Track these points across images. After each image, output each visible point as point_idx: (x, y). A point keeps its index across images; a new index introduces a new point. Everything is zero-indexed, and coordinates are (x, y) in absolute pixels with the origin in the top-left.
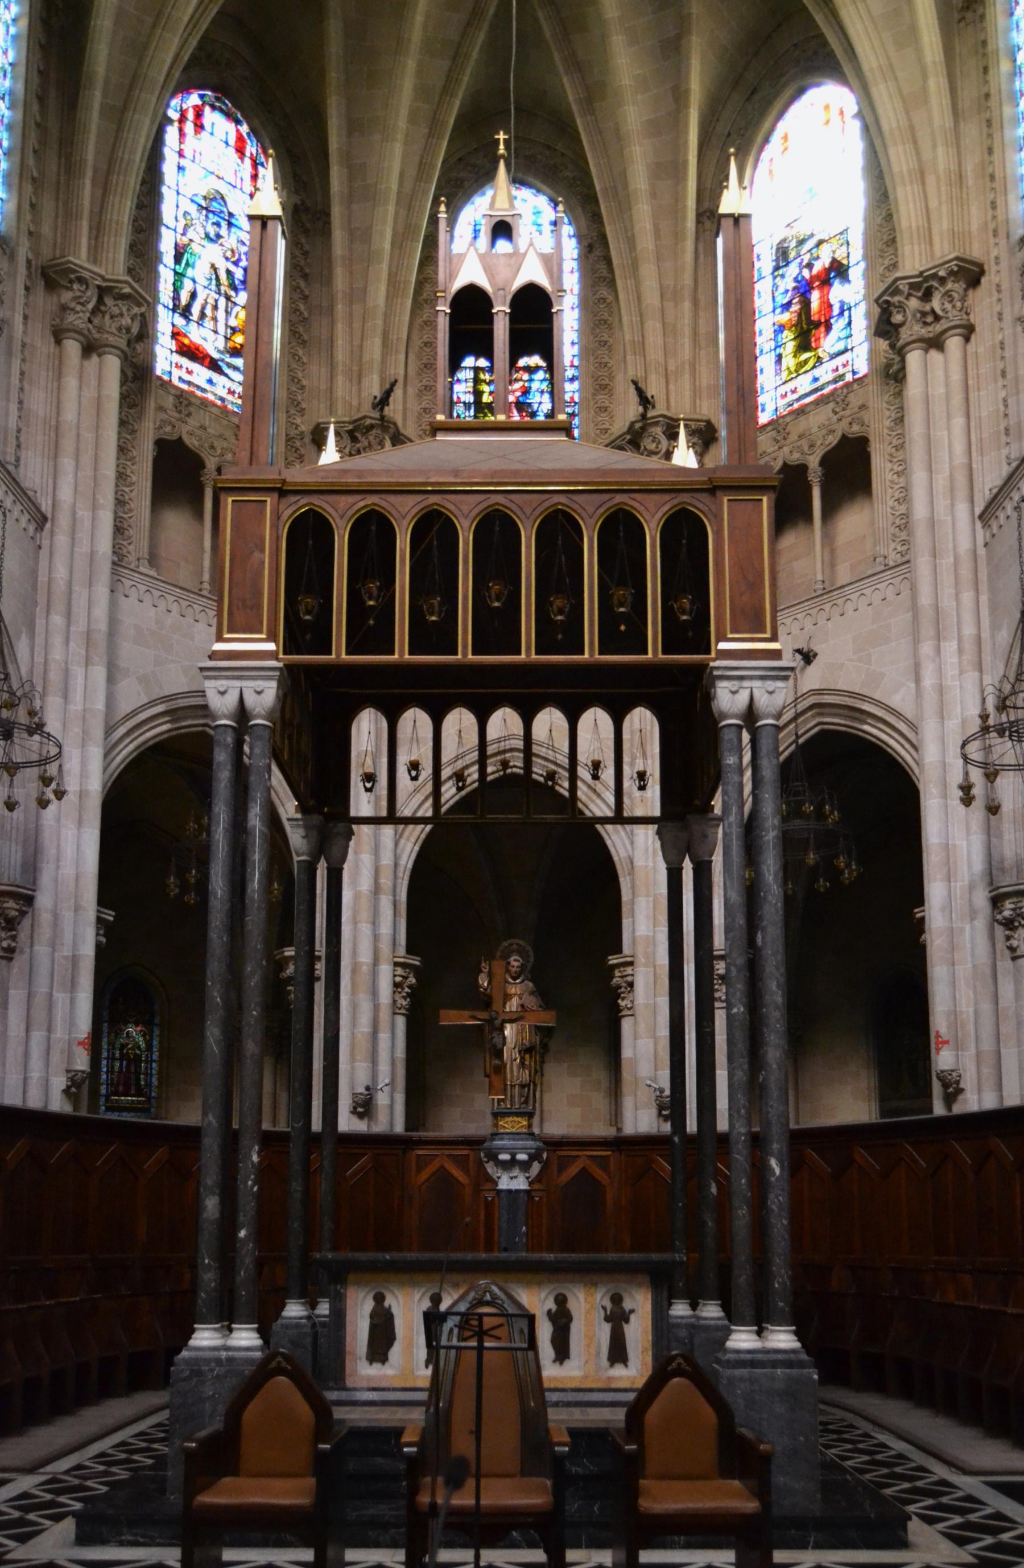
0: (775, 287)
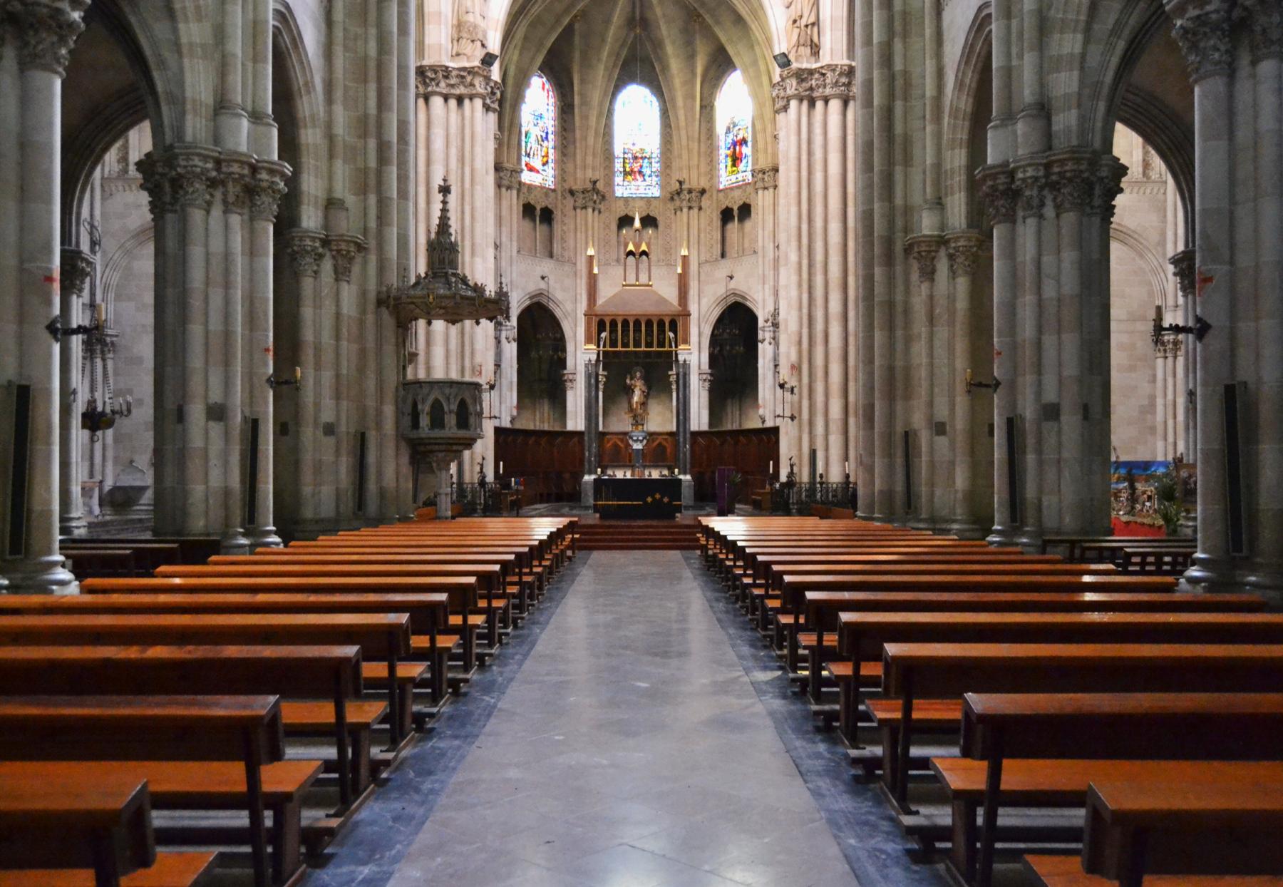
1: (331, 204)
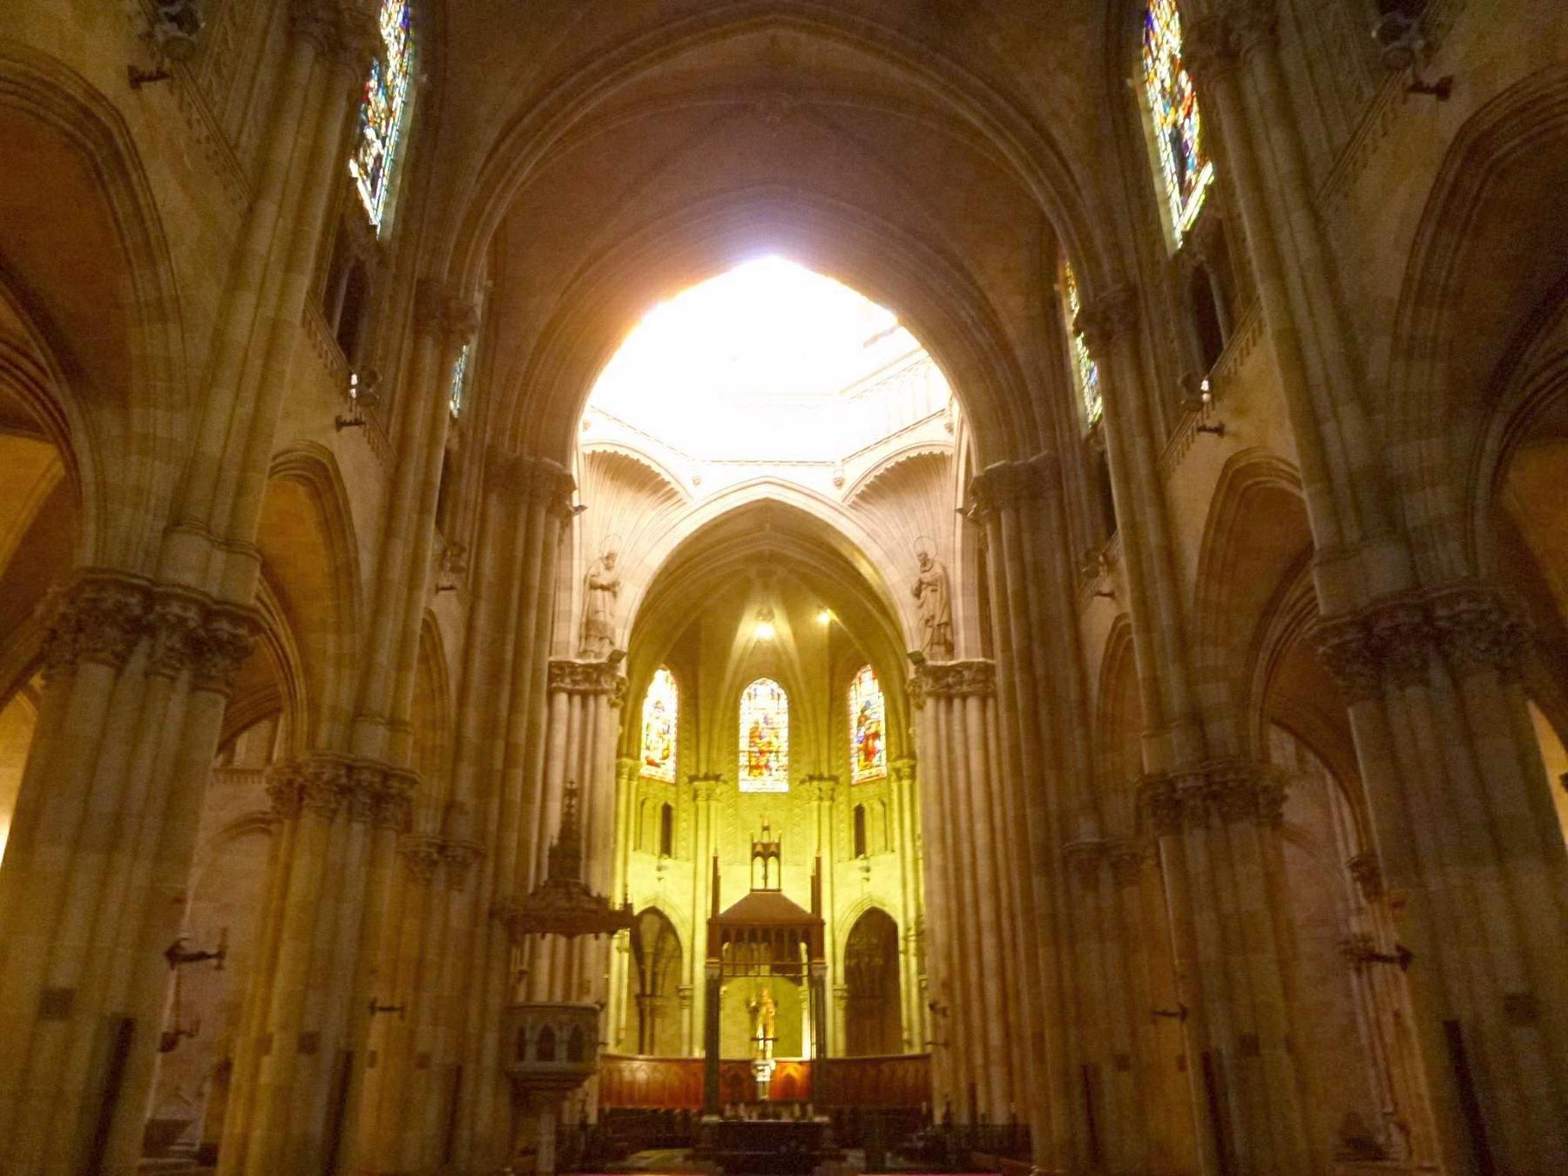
1: (451, 807)
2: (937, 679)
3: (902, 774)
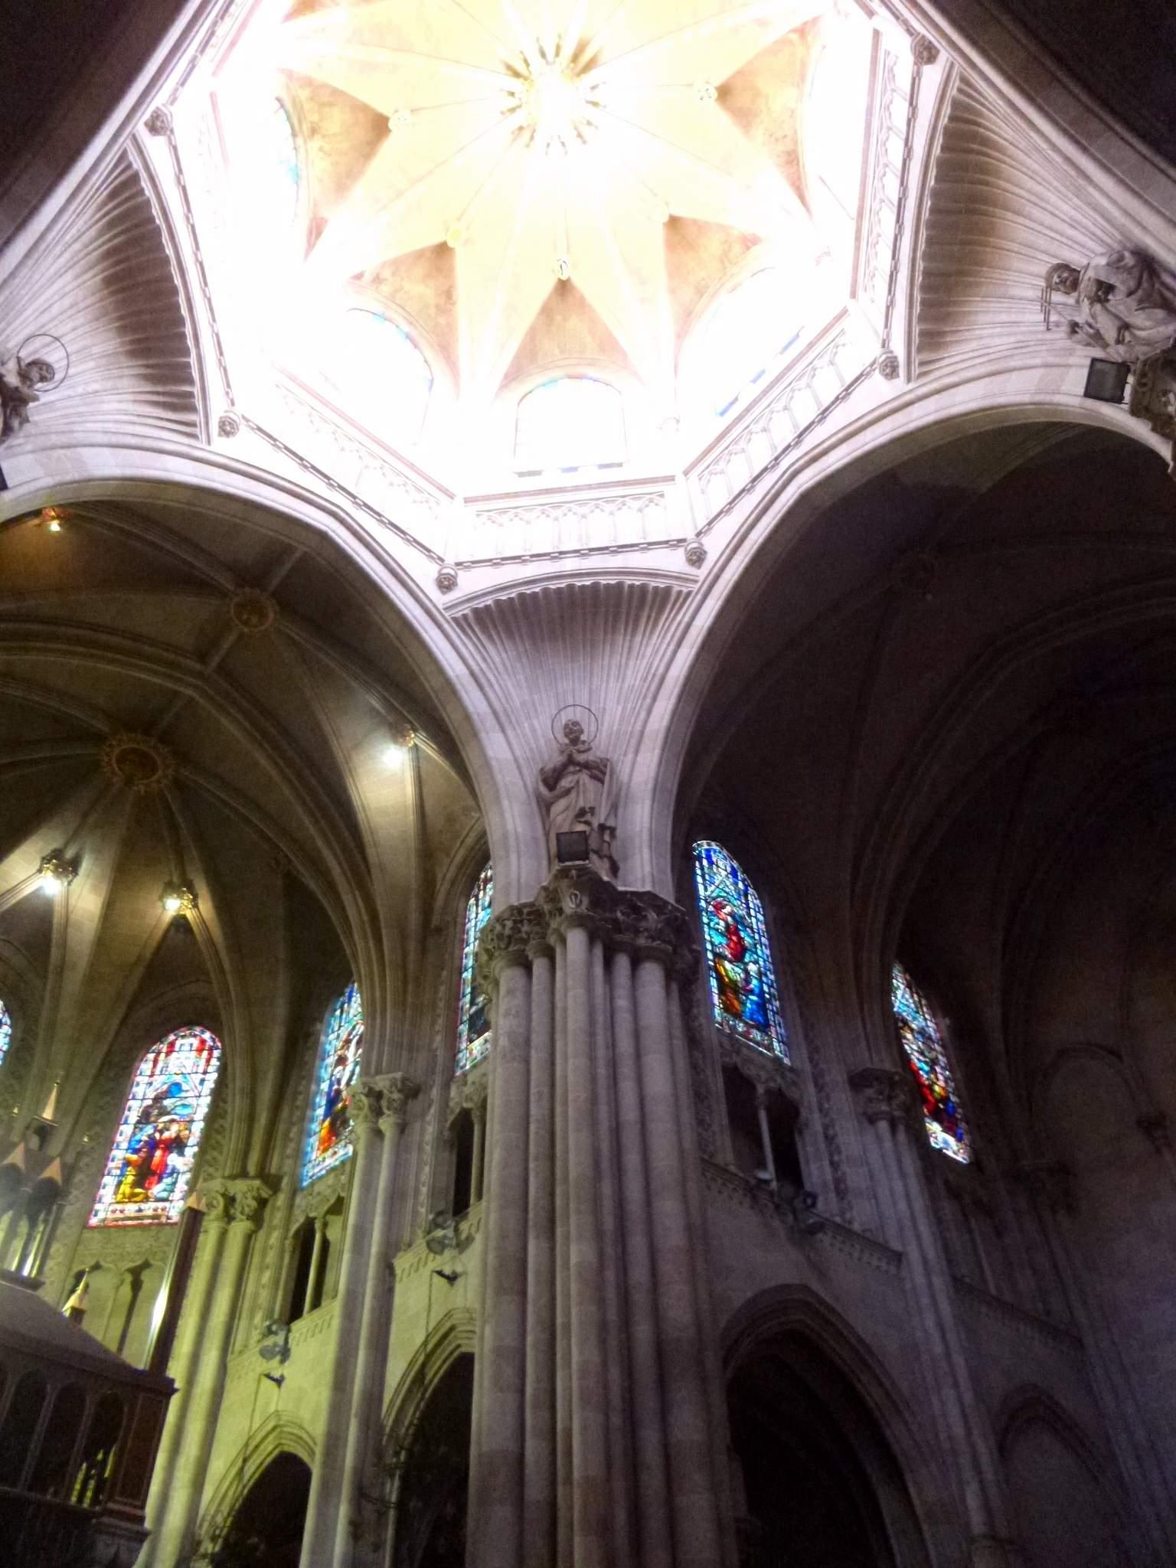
0: (134, 1134)
2: (595, 904)
3: (236, 1211)
